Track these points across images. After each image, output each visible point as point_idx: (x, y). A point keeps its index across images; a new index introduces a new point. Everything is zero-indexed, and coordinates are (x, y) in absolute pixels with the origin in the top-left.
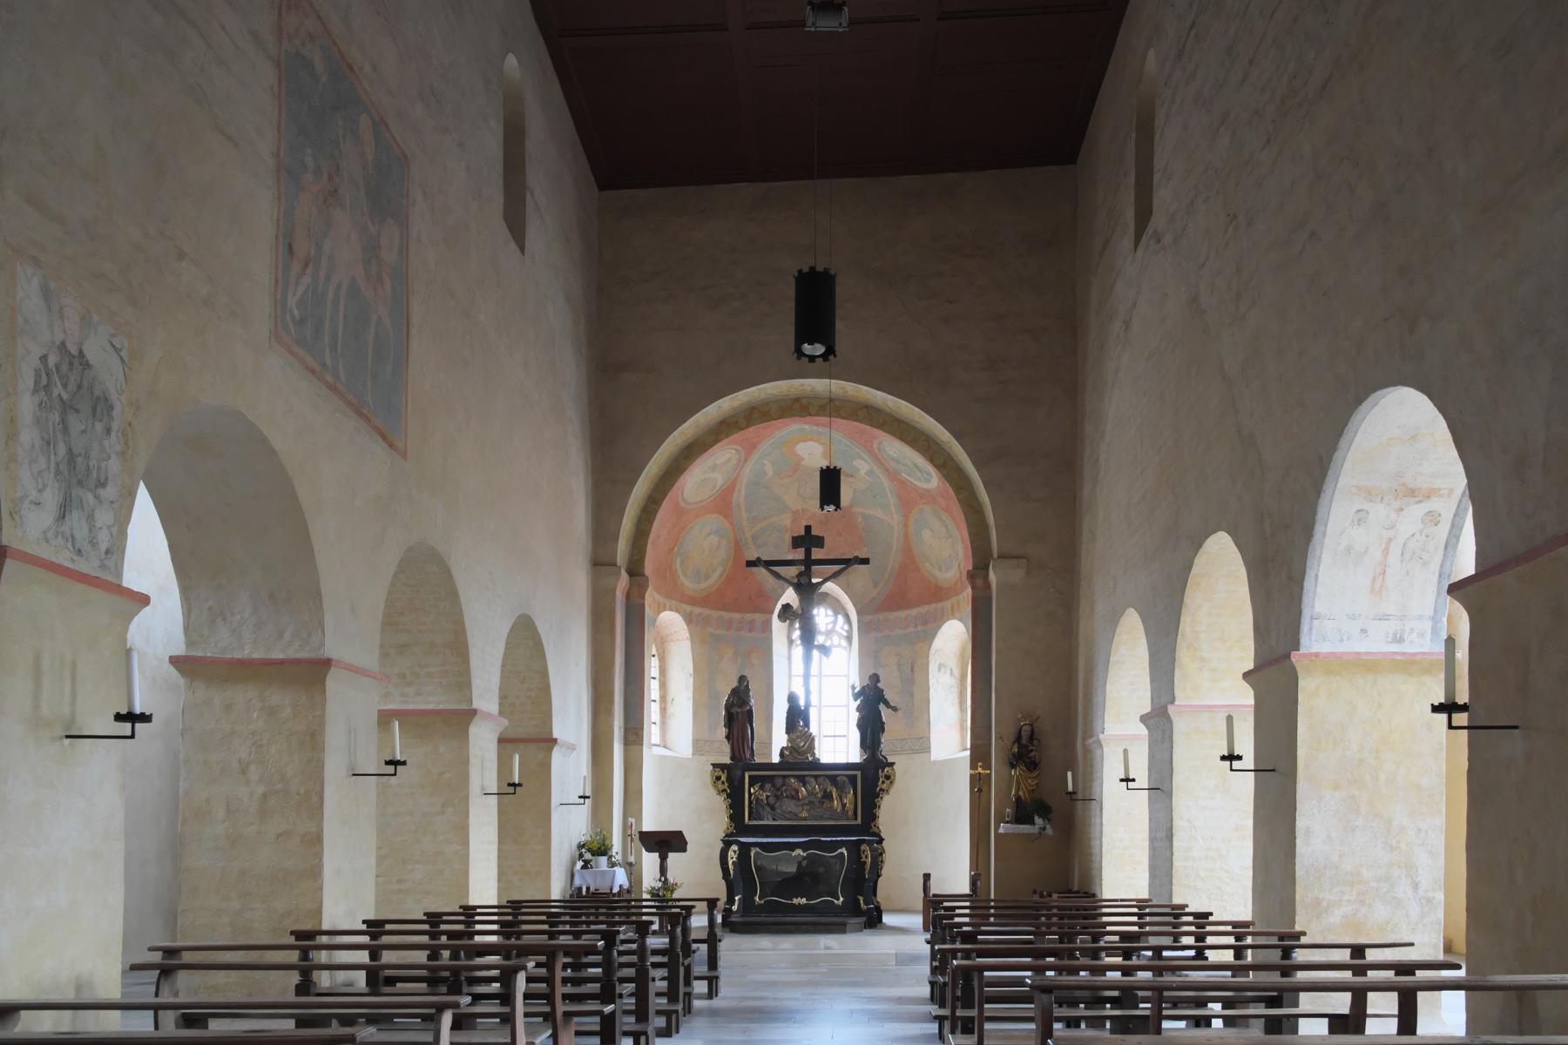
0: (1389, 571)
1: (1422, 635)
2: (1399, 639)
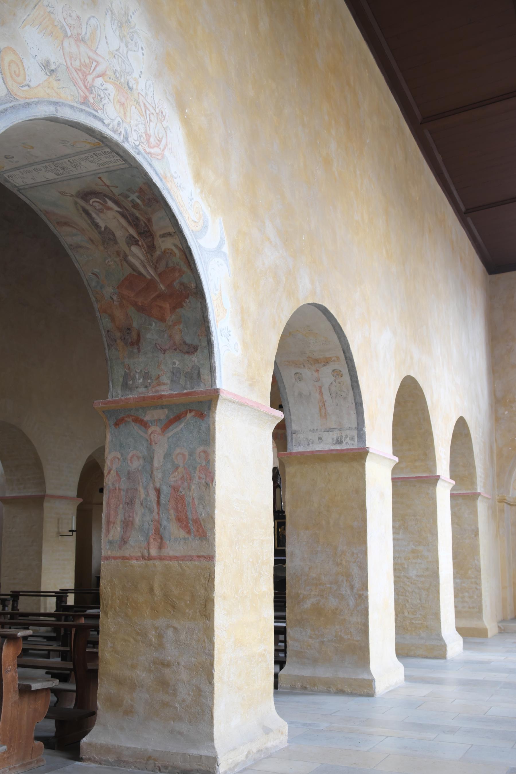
0: (327, 404)
1: (352, 439)
2: (339, 442)
